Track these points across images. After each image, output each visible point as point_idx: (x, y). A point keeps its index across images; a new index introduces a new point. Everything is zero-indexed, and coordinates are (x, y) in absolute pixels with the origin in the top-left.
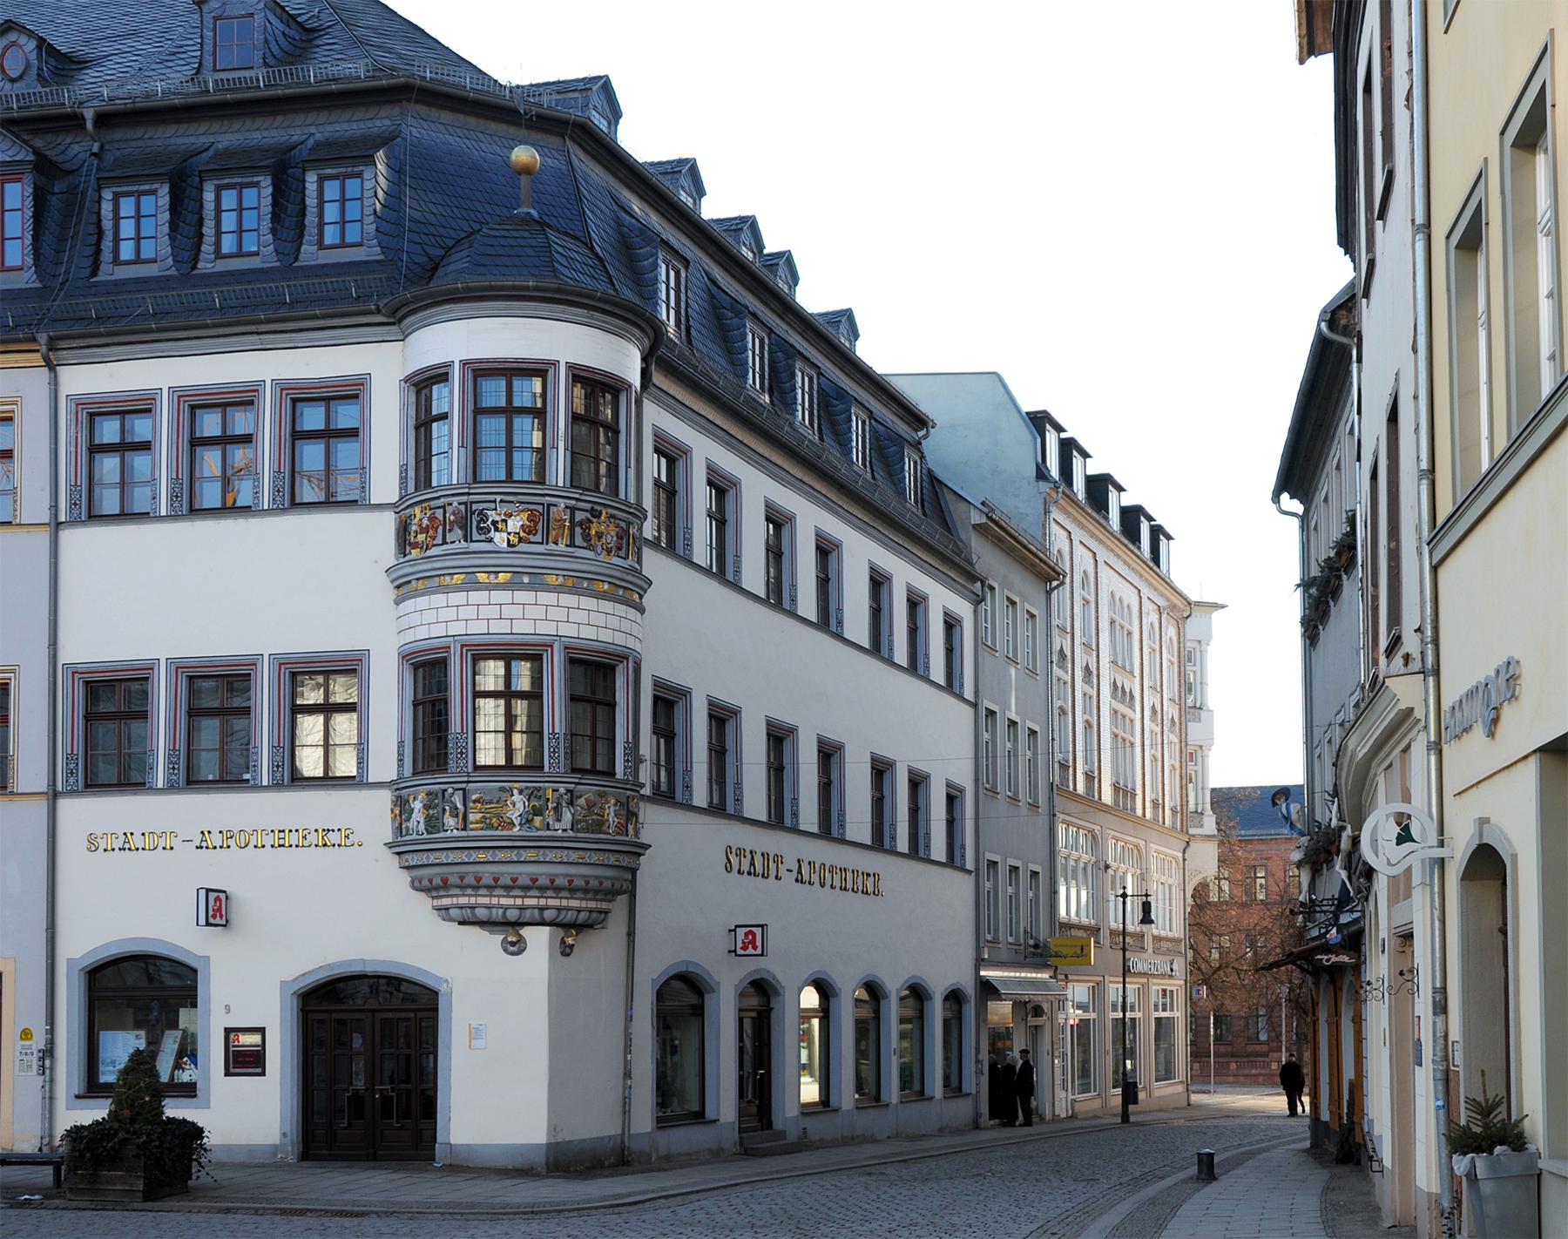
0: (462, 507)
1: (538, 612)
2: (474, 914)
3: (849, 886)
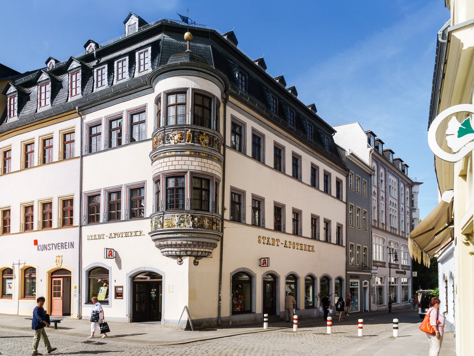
1: (183, 163)
3: (303, 248)
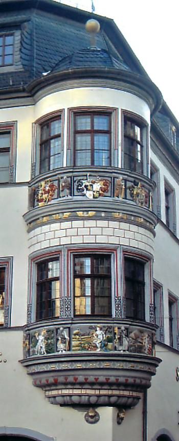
0: (69, 179)
1: (109, 231)
2: (71, 400)
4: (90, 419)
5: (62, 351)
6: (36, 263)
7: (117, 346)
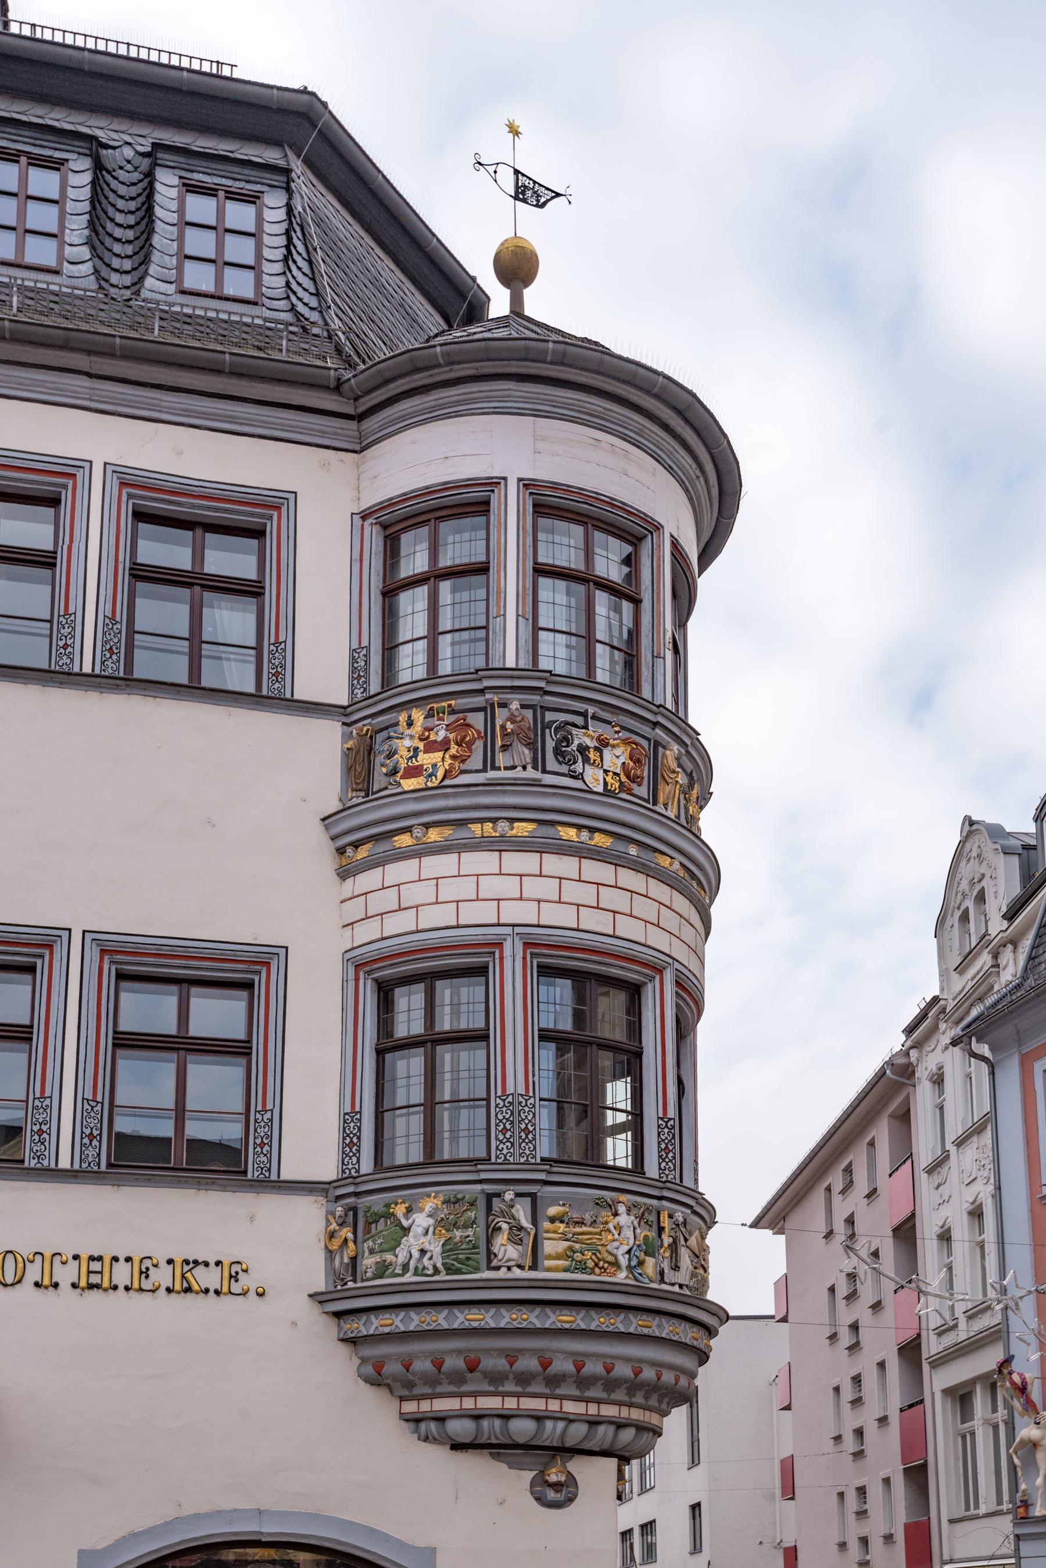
4: (551, 1495)
5: (509, 1268)
6: (376, 980)
7: (666, 1271)
